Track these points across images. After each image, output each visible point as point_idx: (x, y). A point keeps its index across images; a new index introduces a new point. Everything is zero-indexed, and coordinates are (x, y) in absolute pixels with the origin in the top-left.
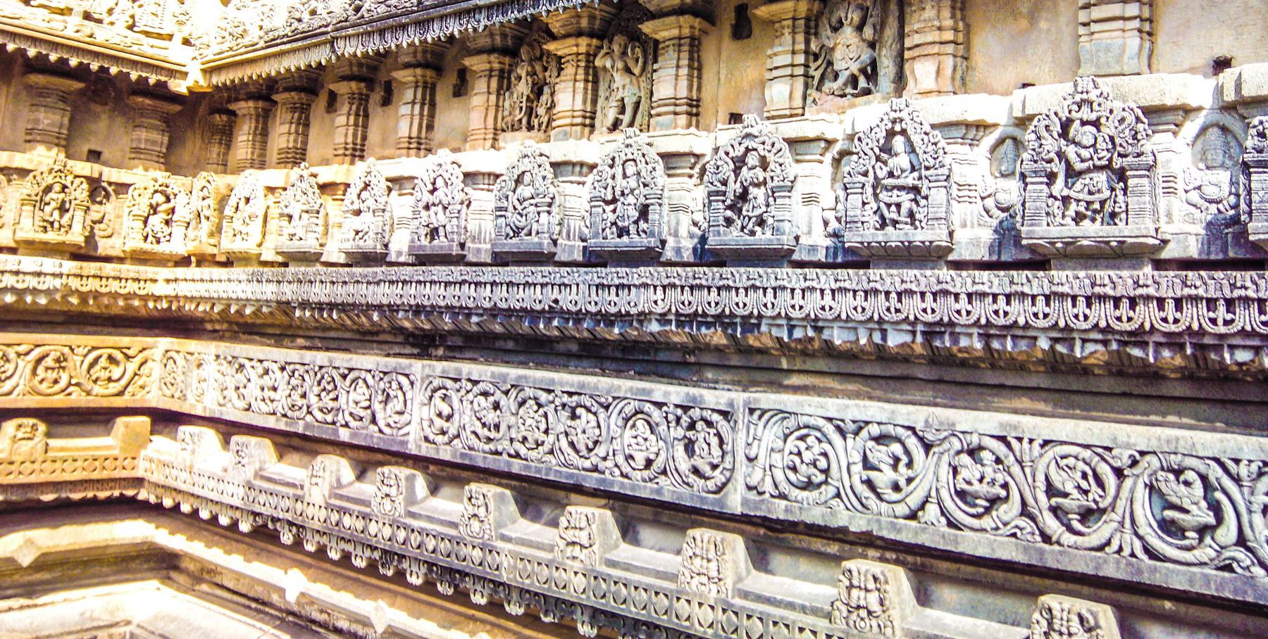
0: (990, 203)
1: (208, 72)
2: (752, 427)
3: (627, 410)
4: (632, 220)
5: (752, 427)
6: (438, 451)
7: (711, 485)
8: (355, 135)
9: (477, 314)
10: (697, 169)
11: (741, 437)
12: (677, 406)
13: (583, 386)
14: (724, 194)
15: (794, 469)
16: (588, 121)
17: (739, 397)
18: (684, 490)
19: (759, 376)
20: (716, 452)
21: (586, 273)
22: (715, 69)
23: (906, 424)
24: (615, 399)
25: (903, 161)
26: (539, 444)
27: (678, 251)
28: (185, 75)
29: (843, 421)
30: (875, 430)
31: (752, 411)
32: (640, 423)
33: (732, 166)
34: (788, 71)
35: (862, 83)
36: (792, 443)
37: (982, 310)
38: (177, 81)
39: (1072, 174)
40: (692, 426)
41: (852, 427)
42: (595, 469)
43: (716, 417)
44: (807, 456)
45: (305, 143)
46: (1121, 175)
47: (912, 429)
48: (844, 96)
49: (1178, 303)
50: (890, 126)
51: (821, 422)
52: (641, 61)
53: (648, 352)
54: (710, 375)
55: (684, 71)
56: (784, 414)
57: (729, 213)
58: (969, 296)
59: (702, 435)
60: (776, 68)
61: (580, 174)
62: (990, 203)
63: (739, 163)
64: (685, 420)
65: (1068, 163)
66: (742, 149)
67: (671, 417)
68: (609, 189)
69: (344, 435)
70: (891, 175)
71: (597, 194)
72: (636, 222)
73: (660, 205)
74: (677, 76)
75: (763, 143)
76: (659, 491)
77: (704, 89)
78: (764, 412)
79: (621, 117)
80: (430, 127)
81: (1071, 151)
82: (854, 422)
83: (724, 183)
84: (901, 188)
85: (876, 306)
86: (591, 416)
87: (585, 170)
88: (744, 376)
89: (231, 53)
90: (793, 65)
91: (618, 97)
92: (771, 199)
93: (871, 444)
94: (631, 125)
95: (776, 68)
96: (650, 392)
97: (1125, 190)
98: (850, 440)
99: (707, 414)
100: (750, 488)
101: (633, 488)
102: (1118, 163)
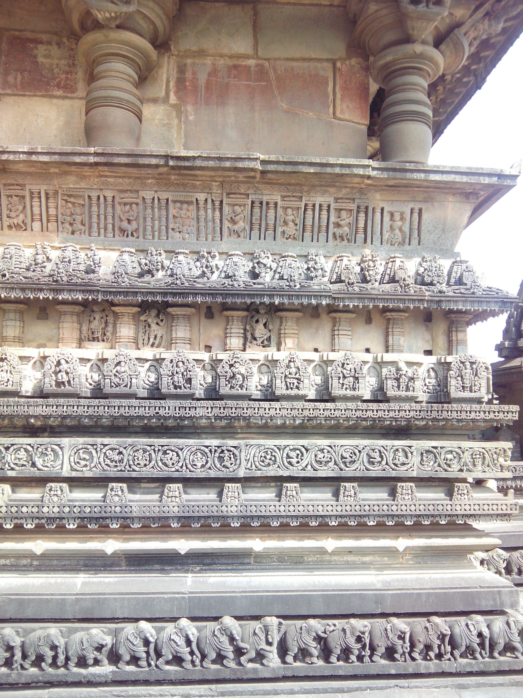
0: (313, 383)
6: (84, 474)
7: (231, 469)
11: (243, 454)
13: (170, 442)
15: (263, 461)
17: (242, 442)
18: (220, 473)
19: (225, 435)
20: (232, 459)
25: (293, 370)
26: (145, 465)
27: (200, 394)
30: (291, 447)
31: (247, 446)
32: (198, 453)
34: (232, 335)
37: (327, 413)
39: (344, 377)
40: (222, 452)
41: (283, 447)
42: (177, 471)
43: (232, 449)
44: (268, 457)
46: (357, 378)
47: (303, 446)
49: (377, 411)
51: (273, 447)
53: (178, 430)
54: (204, 436)
56: (259, 446)
58: (324, 410)
59: (227, 455)
61: (143, 363)
62: (313, 383)
64: (219, 450)
65: (343, 374)
67: (213, 450)
69: (11, 474)
70: (290, 374)
76: (210, 474)
81: (344, 371)
84: (294, 378)
86: (174, 453)
88: (219, 435)
96: (203, 443)
97: (358, 383)
98: (281, 452)
100: (246, 469)
101: (197, 475)
102: (357, 375)
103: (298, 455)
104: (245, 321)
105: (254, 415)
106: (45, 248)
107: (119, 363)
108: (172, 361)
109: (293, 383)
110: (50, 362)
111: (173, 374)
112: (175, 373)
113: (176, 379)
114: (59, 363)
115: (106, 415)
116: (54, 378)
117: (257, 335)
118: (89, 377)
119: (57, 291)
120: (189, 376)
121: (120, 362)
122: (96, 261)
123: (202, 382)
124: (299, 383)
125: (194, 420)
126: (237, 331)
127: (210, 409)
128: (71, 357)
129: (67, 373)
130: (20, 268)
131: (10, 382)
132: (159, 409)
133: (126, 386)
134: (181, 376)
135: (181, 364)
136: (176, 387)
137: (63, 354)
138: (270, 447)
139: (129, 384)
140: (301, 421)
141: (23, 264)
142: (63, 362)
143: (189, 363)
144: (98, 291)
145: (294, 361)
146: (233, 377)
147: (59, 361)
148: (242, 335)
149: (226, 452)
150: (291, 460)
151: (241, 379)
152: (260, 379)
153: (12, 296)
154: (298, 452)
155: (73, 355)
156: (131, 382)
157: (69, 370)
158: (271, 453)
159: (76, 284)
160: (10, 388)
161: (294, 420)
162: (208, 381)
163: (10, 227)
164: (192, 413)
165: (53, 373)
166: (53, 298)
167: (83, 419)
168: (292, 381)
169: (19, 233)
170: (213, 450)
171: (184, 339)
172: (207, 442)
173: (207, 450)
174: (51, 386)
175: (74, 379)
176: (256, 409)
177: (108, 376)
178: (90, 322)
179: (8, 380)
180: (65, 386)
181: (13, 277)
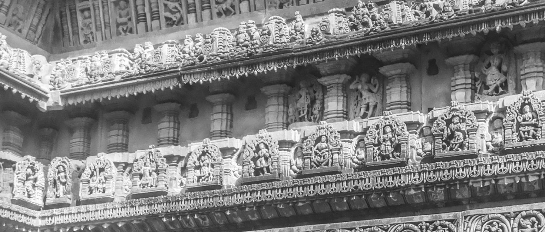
1: (65, 97)
2: (466, 223)
3: (399, 228)
4: (390, 152)
5: (466, 223)
8: (174, 133)
9: (301, 202)
10: (419, 131)
12: (426, 222)
14: (442, 135)
16: (345, 116)
17: (460, 214)
21: (374, 173)
22: (419, 89)
23: (538, 209)
24: (391, 225)
28: (47, 99)
29: (509, 213)
30: (524, 214)
33: (445, 123)
35: (501, 90)
36: (485, 226)
38: (43, 102)
41: (513, 214)
43: (447, 223)
45: (127, 141)
48: (492, 95)
50: (523, 101)
51: (499, 215)
52: (377, 87)
55: (405, 89)
57: (444, 143)
60: (457, 85)
63: (449, 122)
66: (451, 116)
67: (424, 227)
68: (376, 139)
71: (370, 141)
72: (392, 153)
73: (407, 143)
74: (401, 91)
75: (461, 113)
77: (413, 98)
78: (472, 216)
79: (367, 112)
80: (231, 126)
82: (514, 212)
83: (442, 130)
85: (525, 166)
87: (352, 136)
89: (88, 85)
90: (466, 84)
91: (367, 102)
92: (467, 136)
93: (522, 219)
94: (372, 116)
95: (457, 85)
98: (512, 221)
99: (443, 222)
103: (533, 223)
104: (472, 67)
105: (472, 176)
106: (249, 27)
107: (319, 140)
108: (378, 127)
109: (528, 132)
110: (249, 148)
111: (378, 141)
112: (381, 141)
113: (383, 147)
114: (258, 149)
115: (301, 196)
116: (253, 165)
117: (489, 83)
118: (294, 162)
119: (252, 65)
120: (397, 142)
121: (321, 137)
122: (297, 28)
123: (420, 151)
124: (536, 131)
125: (401, 192)
126: (463, 81)
127: (417, 175)
128: (269, 139)
129: (266, 159)
130: (224, 53)
131: (211, 176)
132: (358, 183)
133: (327, 164)
134: (389, 143)
135: (388, 129)
136: (383, 157)
137: (262, 137)
138: (495, 215)
139: (330, 160)
140: (537, 178)
141: (227, 47)
142: (262, 146)
143: (398, 125)
144: (293, 57)
145: (529, 104)
146: (452, 136)
147: (258, 145)
148: (470, 86)
149: (439, 228)
150: (523, 230)
151: (461, 136)
152: (493, 137)
153: (210, 80)
154: (534, 219)
155: (272, 137)
156: (332, 158)
157: (268, 155)
158: (498, 223)
159: (269, 54)
160: (211, 182)
161: (527, 177)
162: (426, 149)
163: (219, 14)
164: (396, 182)
165: (251, 160)
166: (249, 74)
167: (278, 206)
168: (527, 128)
169: (228, 18)
170: (424, 227)
171: (400, 103)
172: (416, 218)
173: (416, 228)
174: (249, 175)
175: (272, 163)
176: (475, 168)
177: (307, 154)
178: (297, 101)
179: (209, 174)
180: (263, 173)
181: (210, 59)
